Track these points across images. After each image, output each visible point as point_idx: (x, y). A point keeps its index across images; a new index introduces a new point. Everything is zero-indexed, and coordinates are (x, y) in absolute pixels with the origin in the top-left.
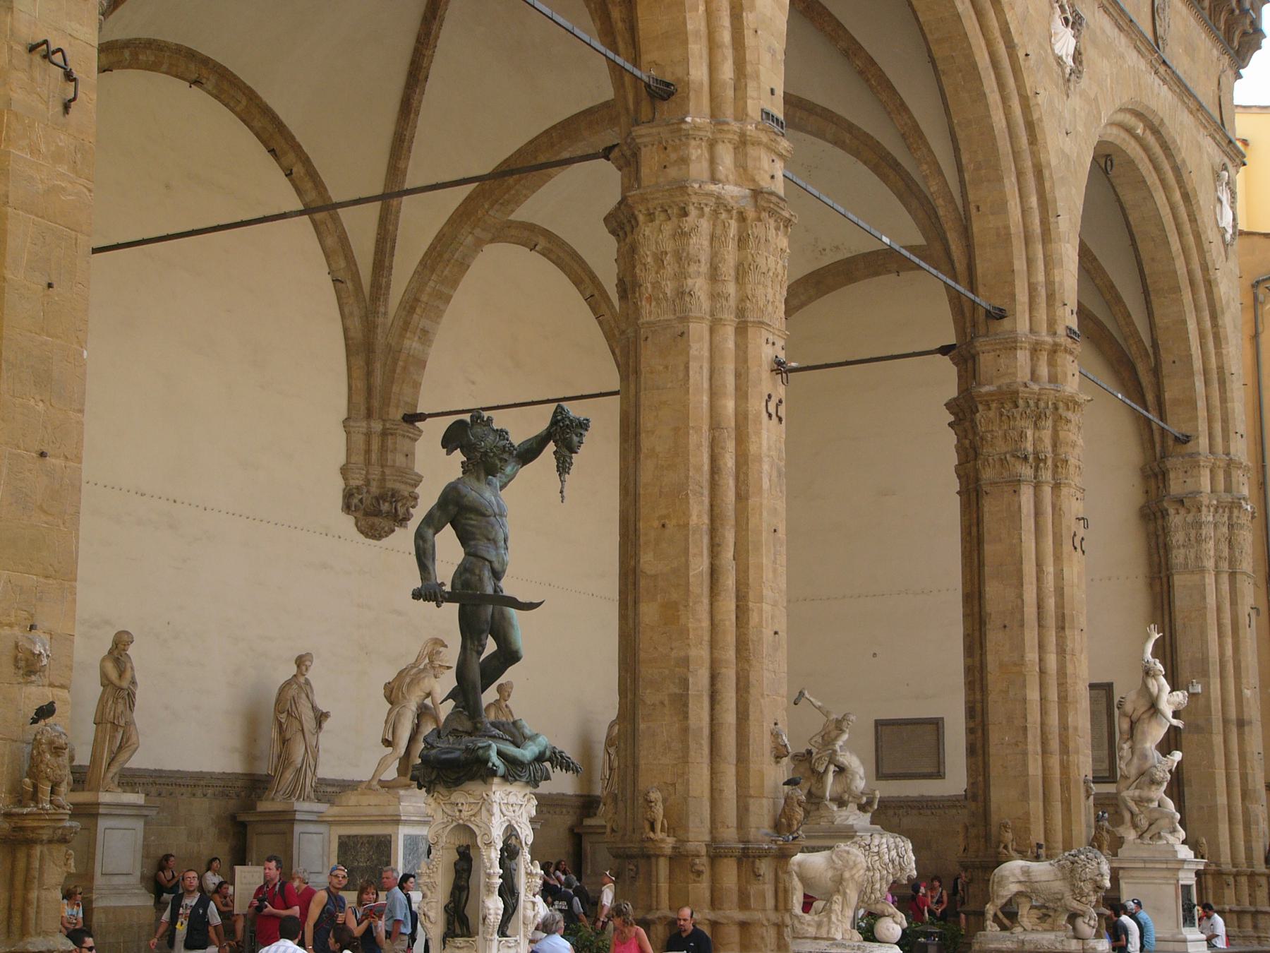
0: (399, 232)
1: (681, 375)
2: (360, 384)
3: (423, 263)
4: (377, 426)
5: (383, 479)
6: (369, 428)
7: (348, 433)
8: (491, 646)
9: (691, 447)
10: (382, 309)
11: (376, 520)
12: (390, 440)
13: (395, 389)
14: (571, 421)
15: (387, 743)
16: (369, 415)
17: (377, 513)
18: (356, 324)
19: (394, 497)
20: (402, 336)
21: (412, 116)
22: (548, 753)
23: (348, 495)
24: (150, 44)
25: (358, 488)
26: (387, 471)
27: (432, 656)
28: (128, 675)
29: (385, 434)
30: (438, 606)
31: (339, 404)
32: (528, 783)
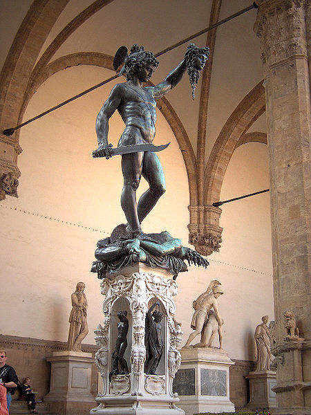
1: (293, 86)
2: (194, 192)
3: (217, 141)
4: (202, 208)
8: (144, 186)
9: (301, 121)
15: (194, 327)
16: (198, 204)
19: (209, 236)
20: (211, 171)
22: (184, 253)
23: (191, 237)
24: (97, 55)
27: (214, 289)
28: (82, 300)
29: (205, 211)
32: (168, 270)
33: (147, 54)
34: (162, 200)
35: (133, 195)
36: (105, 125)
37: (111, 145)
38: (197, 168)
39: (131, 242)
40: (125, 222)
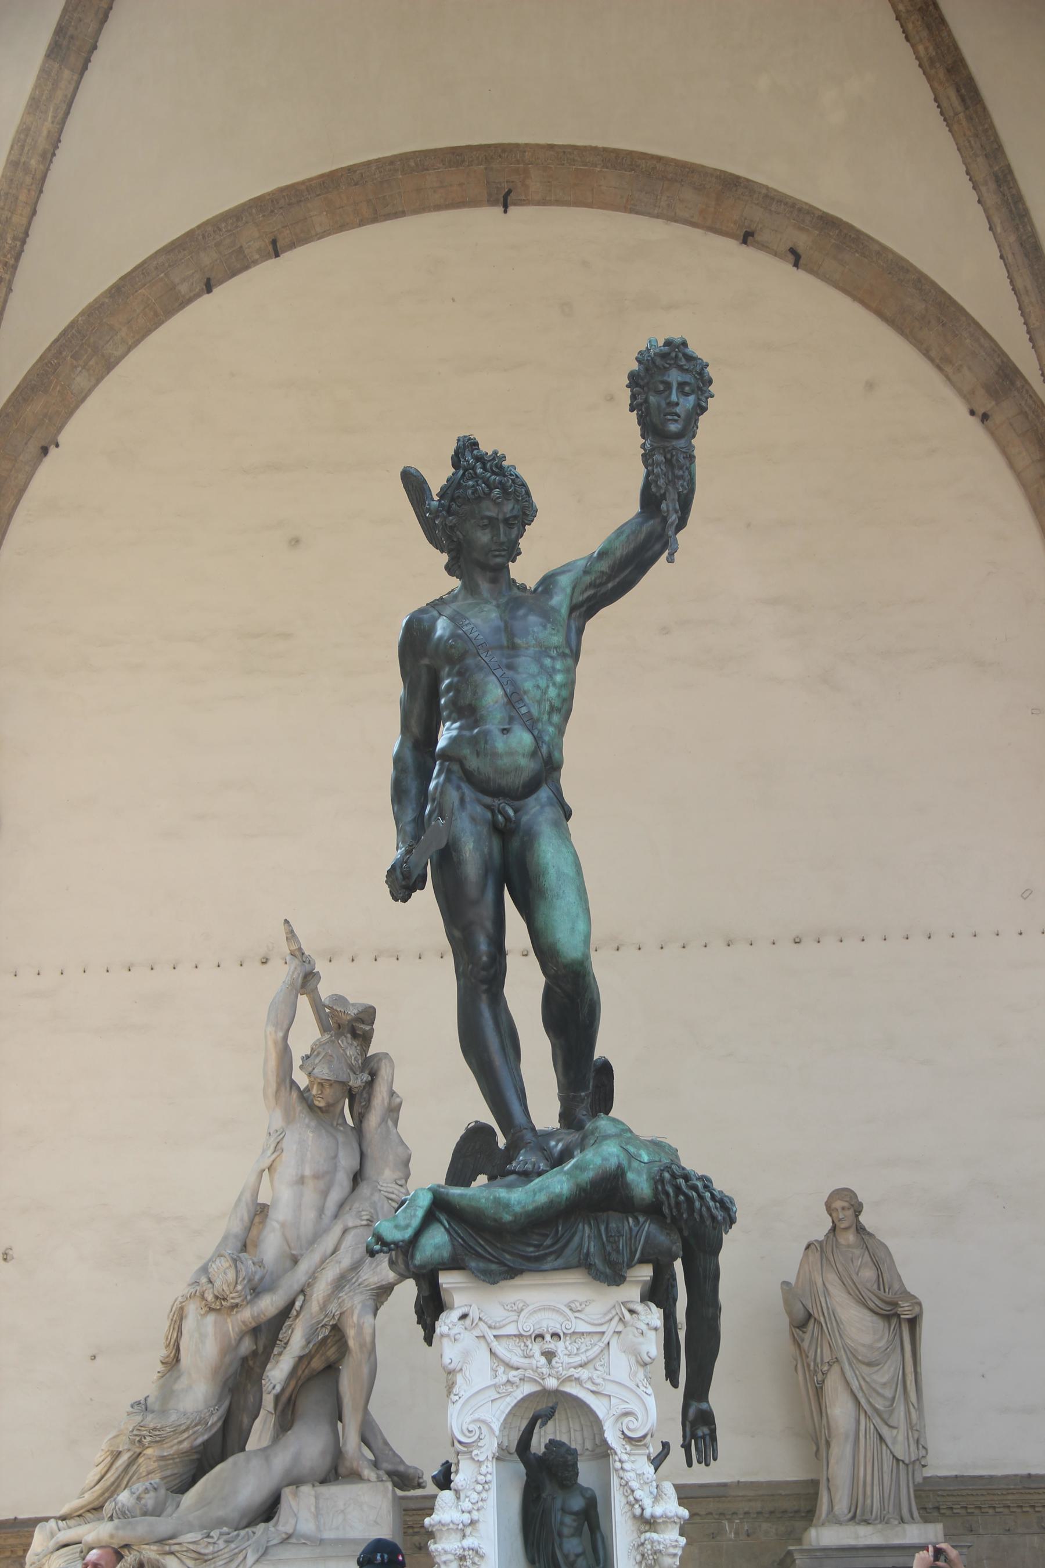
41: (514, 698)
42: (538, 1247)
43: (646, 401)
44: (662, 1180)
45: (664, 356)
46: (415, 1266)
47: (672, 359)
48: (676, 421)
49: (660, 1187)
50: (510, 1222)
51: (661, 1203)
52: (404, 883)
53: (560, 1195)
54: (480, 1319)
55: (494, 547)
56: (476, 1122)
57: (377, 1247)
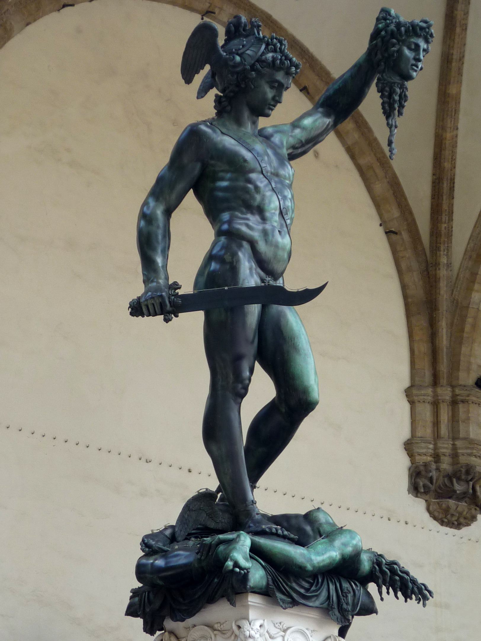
0: (458, 171)
2: (423, 348)
4: (445, 393)
5: (455, 455)
6: (435, 395)
7: (412, 403)
8: (261, 391)
10: (444, 260)
11: (452, 502)
12: (461, 408)
13: (465, 350)
14: (399, 25)
16: (435, 382)
17: (450, 494)
18: (415, 279)
20: (469, 290)
21: (458, 30)
22: (366, 565)
25: (426, 465)
26: (458, 443)
29: (454, 403)
30: (167, 320)
31: (400, 372)
33: (267, 45)
34: (307, 427)
35: (234, 415)
36: (160, 233)
37: (176, 286)
38: (430, 281)
39: (229, 542)
40: (212, 484)
41: (284, 211)
42: (307, 590)
43: (400, 52)
44: (379, 564)
45: (422, 28)
46: (250, 586)
47: (425, 32)
48: (416, 71)
49: (377, 567)
50: (310, 571)
51: (378, 578)
52: (171, 309)
53: (334, 560)
54: (267, 632)
55: (272, 103)
56: (207, 489)
57: (237, 570)
